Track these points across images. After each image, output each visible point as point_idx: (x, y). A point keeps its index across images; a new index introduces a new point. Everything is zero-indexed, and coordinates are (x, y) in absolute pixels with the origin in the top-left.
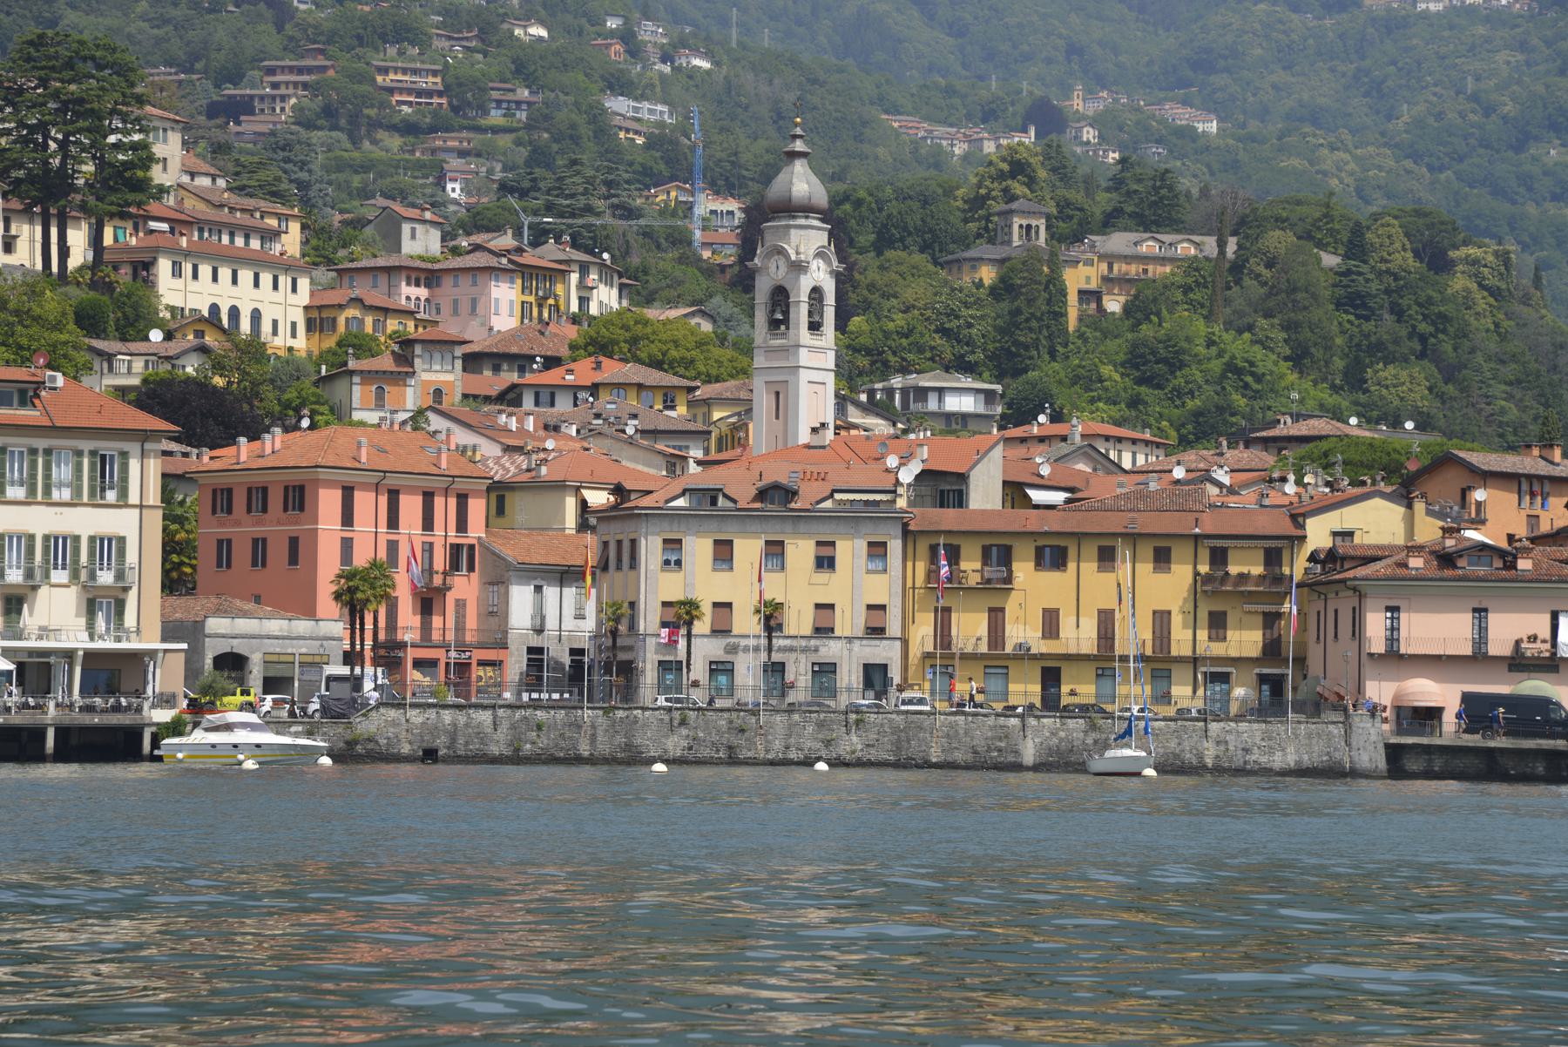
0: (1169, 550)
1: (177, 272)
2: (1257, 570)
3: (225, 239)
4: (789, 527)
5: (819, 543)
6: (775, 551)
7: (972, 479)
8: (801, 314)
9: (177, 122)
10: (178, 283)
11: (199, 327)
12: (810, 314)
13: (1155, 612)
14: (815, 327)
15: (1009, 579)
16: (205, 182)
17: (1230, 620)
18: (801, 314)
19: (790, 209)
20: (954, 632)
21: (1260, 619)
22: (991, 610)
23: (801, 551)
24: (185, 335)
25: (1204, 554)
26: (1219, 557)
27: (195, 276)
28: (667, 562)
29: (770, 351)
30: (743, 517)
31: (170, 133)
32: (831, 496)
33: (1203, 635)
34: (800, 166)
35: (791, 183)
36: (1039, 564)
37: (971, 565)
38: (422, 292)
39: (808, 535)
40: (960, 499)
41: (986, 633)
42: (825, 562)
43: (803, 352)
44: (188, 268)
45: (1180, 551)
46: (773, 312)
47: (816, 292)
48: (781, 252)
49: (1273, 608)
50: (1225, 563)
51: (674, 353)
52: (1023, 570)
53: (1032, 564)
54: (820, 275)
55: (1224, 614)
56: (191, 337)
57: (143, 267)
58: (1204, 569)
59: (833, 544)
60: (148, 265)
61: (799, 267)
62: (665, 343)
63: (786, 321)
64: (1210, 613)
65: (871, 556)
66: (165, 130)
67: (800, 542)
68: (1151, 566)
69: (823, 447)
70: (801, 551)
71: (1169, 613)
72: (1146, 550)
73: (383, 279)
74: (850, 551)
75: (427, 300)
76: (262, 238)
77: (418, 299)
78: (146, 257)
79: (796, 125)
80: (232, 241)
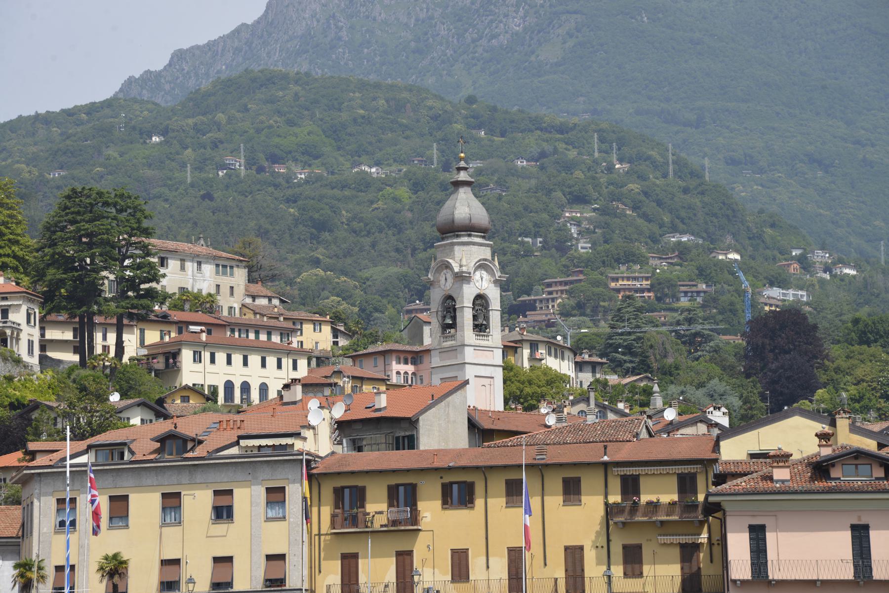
0: (578, 481)
1: (197, 358)
2: (670, 496)
3: (252, 336)
4: (185, 477)
5: (217, 493)
6: (172, 502)
7: (421, 423)
8: (466, 317)
9: (241, 261)
10: (199, 367)
11: (185, 394)
12: (475, 317)
13: (567, 548)
14: (481, 328)
15: (414, 519)
16: (264, 302)
17: (646, 553)
18: (466, 317)
19: (453, 230)
20: (362, 579)
21: (677, 552)
22: (399, 554)
23: (198, 502)
24: (174, 400)
25: (615, 484)
26: (631, 486)
27: (213, 361)
28: (62, 524)
29: (443, 351)
30: (141, 470)
31: (235, 269)
32: (237, 443)
33: (618, 570)
34: (464, 194)
35: (454, 207)
36: (447, 501)
37: (377, 507)
38: (410, 368)
39: (205, 484)
40: (411, 442)
41: (393, 579)
42: (223, 512)
43: (468, 351)
44: (206, 356)
45: (590, 481)
46: (444, 317)
47: (481, 300)
48: (448, 266)
49: (688, 539)
50: (637, 493)
51: (528, 390)
52: (430, 509)
53: (439, 503)
54: (483, 283)
55: (639, 547)
56: (179, 401)
57: (172, 356)
58: (615, 498)
59: (230, 492)
60: (175, 355)
61: (462, 278)
62: (523, 383)
63: (453, 326)
64: (625, 547)
65: (269, 503)
66: (232, 267)
67: (197, 493)
68: (560, 499)
69: (294, 403)
70: (198, 502)
71: (581, 548)
72: (555, 482)
73: (380, 361)
74: (248, 498)
75: (414, 374)
76: (281, 334)
77: (406, 373)
78: (173, 349)
79: (461, 159)
80: (257, 337)
